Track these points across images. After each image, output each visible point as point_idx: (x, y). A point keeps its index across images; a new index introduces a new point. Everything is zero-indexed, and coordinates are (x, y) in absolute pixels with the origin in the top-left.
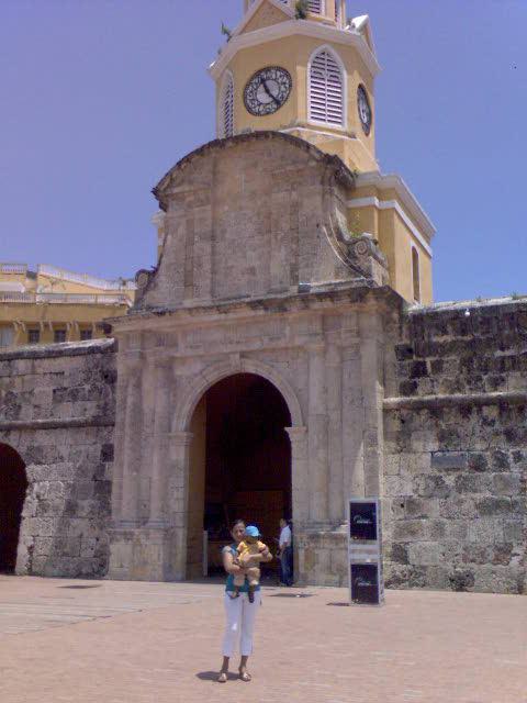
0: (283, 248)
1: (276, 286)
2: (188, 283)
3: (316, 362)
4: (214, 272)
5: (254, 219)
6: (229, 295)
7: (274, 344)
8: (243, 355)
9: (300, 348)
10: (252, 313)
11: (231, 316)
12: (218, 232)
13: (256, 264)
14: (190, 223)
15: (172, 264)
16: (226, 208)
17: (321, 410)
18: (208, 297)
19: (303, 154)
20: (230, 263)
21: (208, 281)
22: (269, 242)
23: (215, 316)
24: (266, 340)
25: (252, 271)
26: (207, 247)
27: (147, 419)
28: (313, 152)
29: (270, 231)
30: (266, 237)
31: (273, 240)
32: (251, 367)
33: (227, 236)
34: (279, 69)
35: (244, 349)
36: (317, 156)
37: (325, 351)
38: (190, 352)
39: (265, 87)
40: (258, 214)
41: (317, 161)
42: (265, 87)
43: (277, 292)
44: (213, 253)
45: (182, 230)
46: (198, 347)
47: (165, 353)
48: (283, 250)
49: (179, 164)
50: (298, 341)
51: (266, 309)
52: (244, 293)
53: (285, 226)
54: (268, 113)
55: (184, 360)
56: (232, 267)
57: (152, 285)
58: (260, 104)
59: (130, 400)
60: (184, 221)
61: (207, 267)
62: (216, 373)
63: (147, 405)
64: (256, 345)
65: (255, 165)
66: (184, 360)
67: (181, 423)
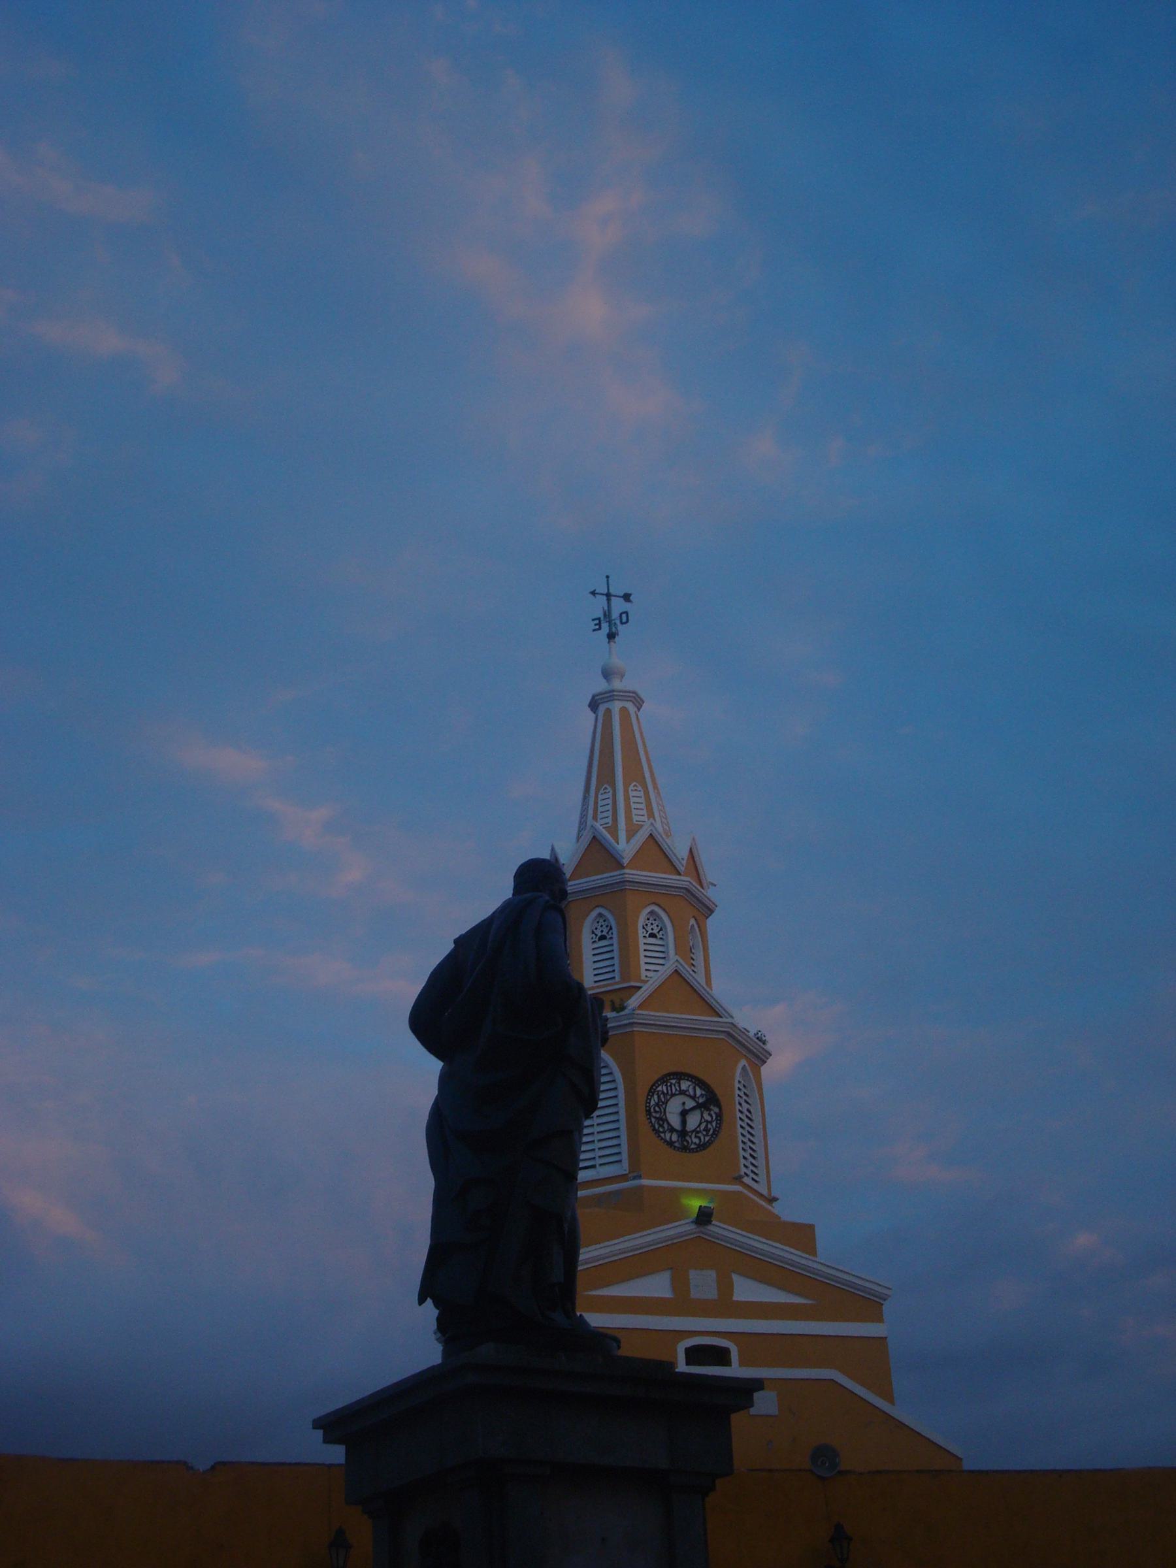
58: (672, 1130)
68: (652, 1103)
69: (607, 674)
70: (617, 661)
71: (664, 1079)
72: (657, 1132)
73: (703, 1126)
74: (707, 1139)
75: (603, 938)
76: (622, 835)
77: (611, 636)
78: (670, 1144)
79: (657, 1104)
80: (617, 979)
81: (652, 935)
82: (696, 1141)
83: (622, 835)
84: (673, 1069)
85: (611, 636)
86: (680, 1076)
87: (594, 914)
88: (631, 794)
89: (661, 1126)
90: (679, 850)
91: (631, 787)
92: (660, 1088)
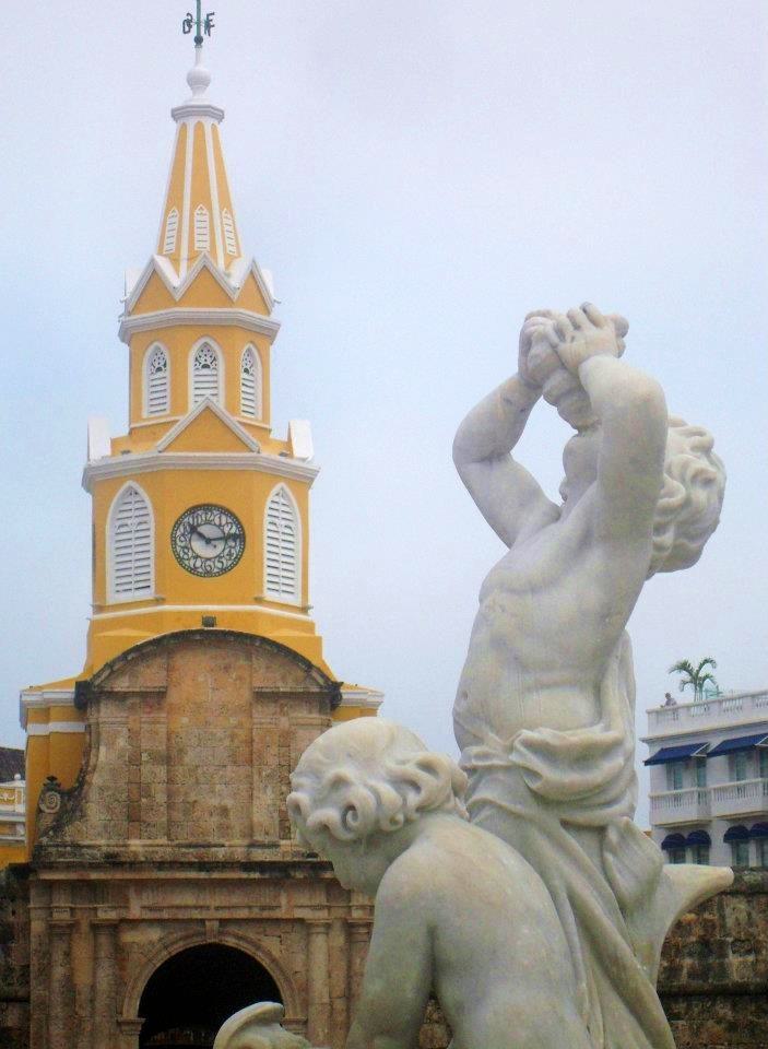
0: (269, 791)
1: (259, 837)
2: (134, 817)
3: (319, 942)
4: (170, 806)
5: (227, 742)
6: (192, 840)
7: (266, 914)
8: (223, 922)
9: (301, 921)
10: (244, 875)
11: (216, 875)
12: (174, 753)
13: (229, 802)
14: (134, 735)
15: (108, 788)
16: (185, 720)
17: (326, 1000)
18: (164, 841)
19: (300, 674)
20: (192, 798)
21: (164, 819)
22: (250, 776)
23: (193, 875)
24: (256, 910)
25: (224, 811)
26: (161, 771)
27: (84, 995)
28: (314, 674)
29: (250, 762)
30: (243, 771)
31: (256, 777)
32: (231, 942)
33: (187, 760)
34: (225, 511)
35: (225, 915)
36: (321, 681)
37: (328, 926)
38: (148, 915)
39: (201, 536)
40: (233, 737)
41: (321, 687)
42: (201, 536)
43: (263, 846)
44: (170, 781)
45: (122, 742)
46: (161, 909)
47: (107, 914)
48: (269, 791)
49: (126, 654)
50: (298, 914)
51: (262, 872)
52: (213, 839)
53: (273, 761)
54: (208, 574)
55: (135, 923)
56: (195, 802)
57: (78, 814)
58: (197, 557)
59: (59, 972)
60: (125, 730)
61: (161, 798)
62: (181, 943)
63: (82, 979)
64: (243, 914)
65: (227, 669)
66: (135, 923)
67: (131, 1010)
68: (178, 533)
69: (197, 82)
70: (203, 69)
71: (193, 510)
72: (180, 560)
73: (227, 551)
74: (230, 563)
75: (159, 369)
76: (184, 265)
77: (199, 40)
78: (193, 570)
79: (183, 535)
80: (168, 412)
81: (206, 366)
82: (220, 565)
83: (184, 265)
84: (202, 502)
85: (199, 40)
86: (207, 507)
87: (152, 348)
88: (197, 218)
89: (185, 553)
90: (236, 279)
91: (197, 211)
92: (186, 520)
